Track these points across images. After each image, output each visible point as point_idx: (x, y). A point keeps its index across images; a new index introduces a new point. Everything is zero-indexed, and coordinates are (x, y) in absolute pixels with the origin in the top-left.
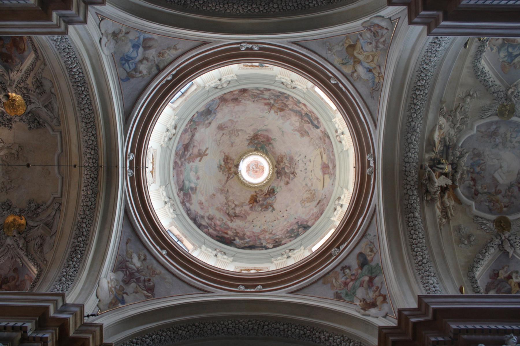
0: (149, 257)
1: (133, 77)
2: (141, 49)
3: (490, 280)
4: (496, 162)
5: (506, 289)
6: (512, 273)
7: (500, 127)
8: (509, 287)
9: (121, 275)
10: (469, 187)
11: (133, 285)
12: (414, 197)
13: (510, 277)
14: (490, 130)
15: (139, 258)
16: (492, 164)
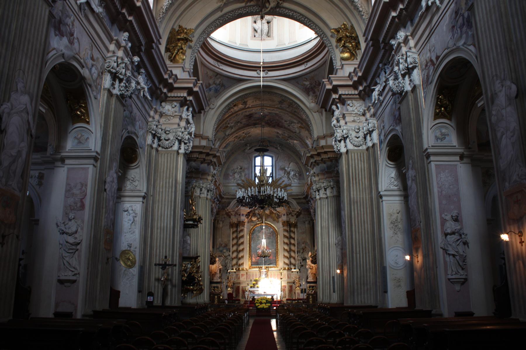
0: (306, 76)
1: (223, 84)
2: (211, 87)
9: (311, 93)
11: (316, 90)
15: (305, 81)
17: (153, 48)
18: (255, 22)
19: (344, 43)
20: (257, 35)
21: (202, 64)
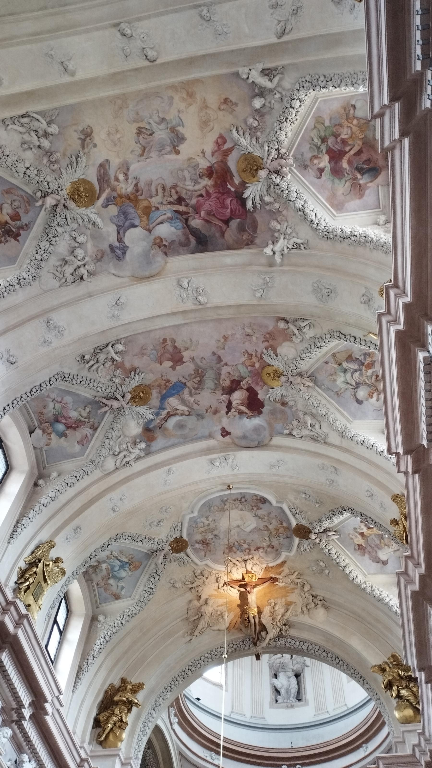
3: (367, 556)
4: (233, 532)
5: (375, 539)
6: (357, 532)
7: (196, 541)
8: (373, 535)
10: (266, 552)
12: (288, 645)
13: (362, 534)
14: (202, 548)
16: (236, 535)
17: (47, 714)
18: (276, 676)
19: (399, 691)
20: (279, 698)
21: (181, 755)
